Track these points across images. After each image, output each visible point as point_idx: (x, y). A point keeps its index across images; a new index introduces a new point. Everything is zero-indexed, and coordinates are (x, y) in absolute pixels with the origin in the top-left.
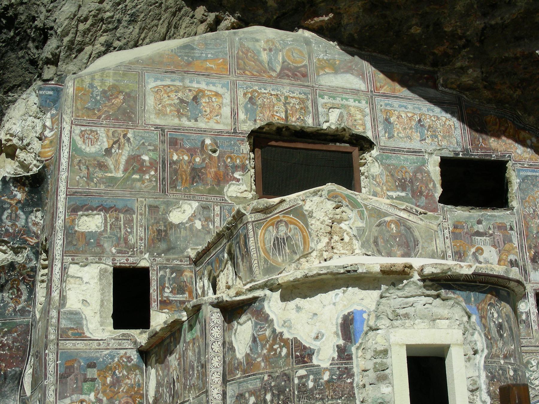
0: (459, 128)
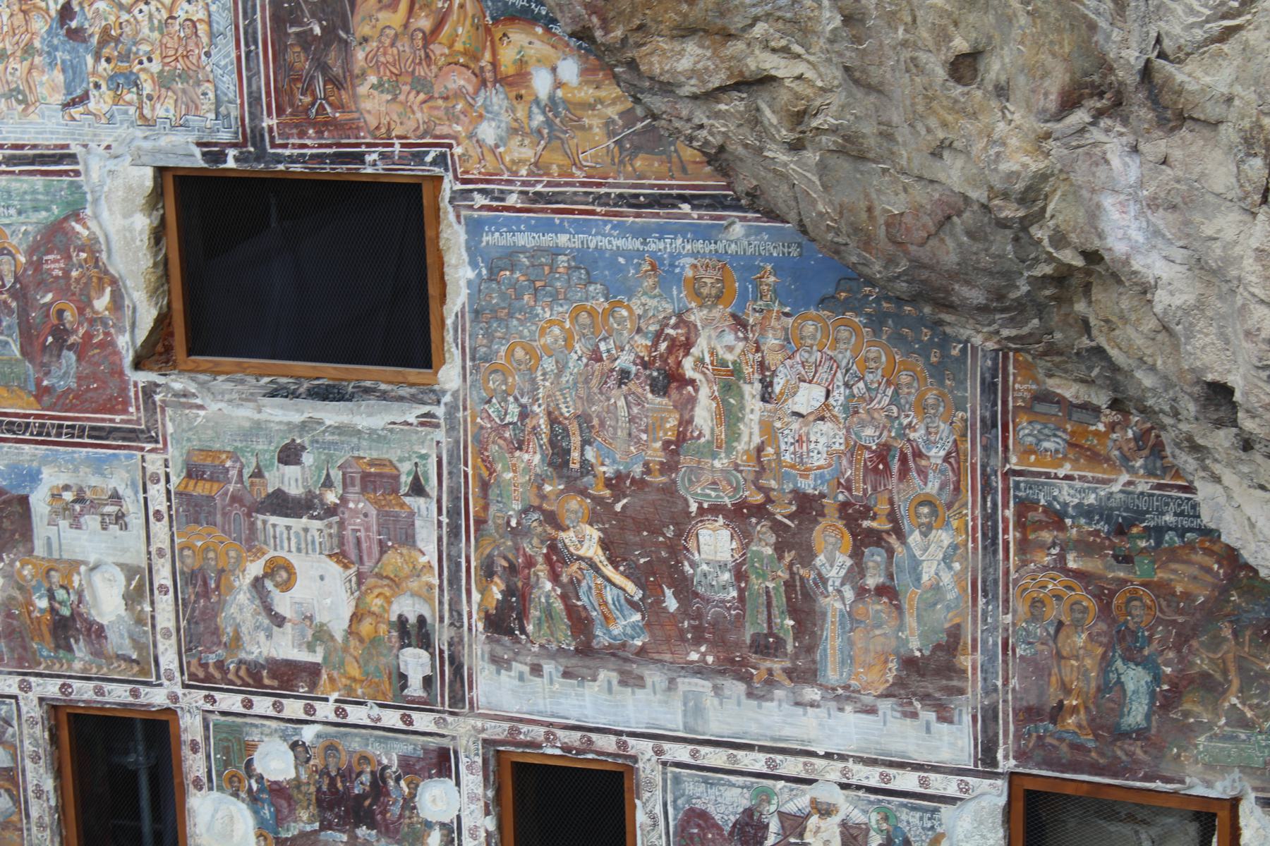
0: (230, 33)
